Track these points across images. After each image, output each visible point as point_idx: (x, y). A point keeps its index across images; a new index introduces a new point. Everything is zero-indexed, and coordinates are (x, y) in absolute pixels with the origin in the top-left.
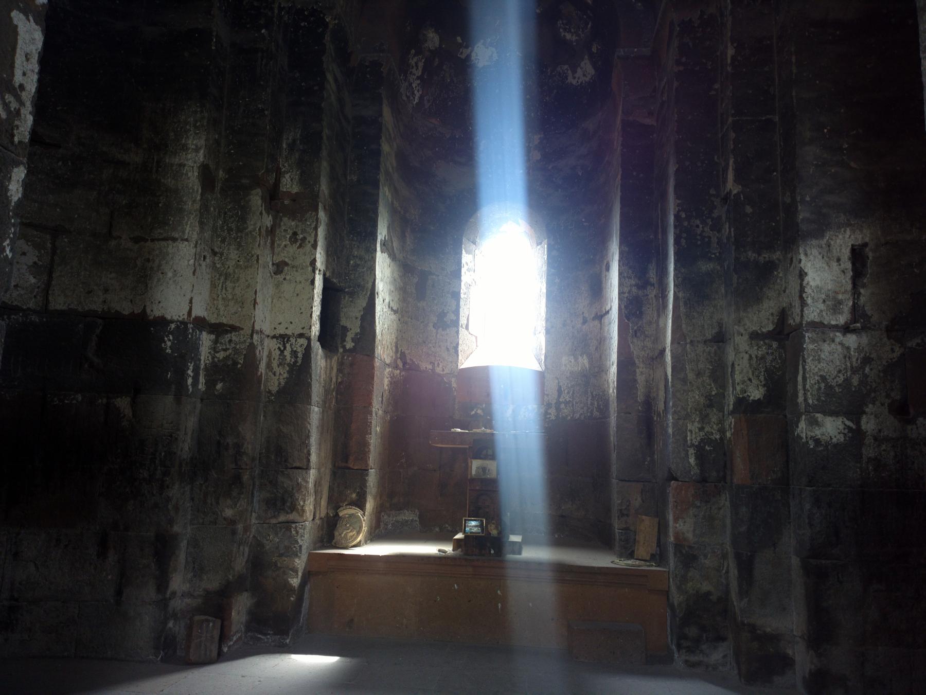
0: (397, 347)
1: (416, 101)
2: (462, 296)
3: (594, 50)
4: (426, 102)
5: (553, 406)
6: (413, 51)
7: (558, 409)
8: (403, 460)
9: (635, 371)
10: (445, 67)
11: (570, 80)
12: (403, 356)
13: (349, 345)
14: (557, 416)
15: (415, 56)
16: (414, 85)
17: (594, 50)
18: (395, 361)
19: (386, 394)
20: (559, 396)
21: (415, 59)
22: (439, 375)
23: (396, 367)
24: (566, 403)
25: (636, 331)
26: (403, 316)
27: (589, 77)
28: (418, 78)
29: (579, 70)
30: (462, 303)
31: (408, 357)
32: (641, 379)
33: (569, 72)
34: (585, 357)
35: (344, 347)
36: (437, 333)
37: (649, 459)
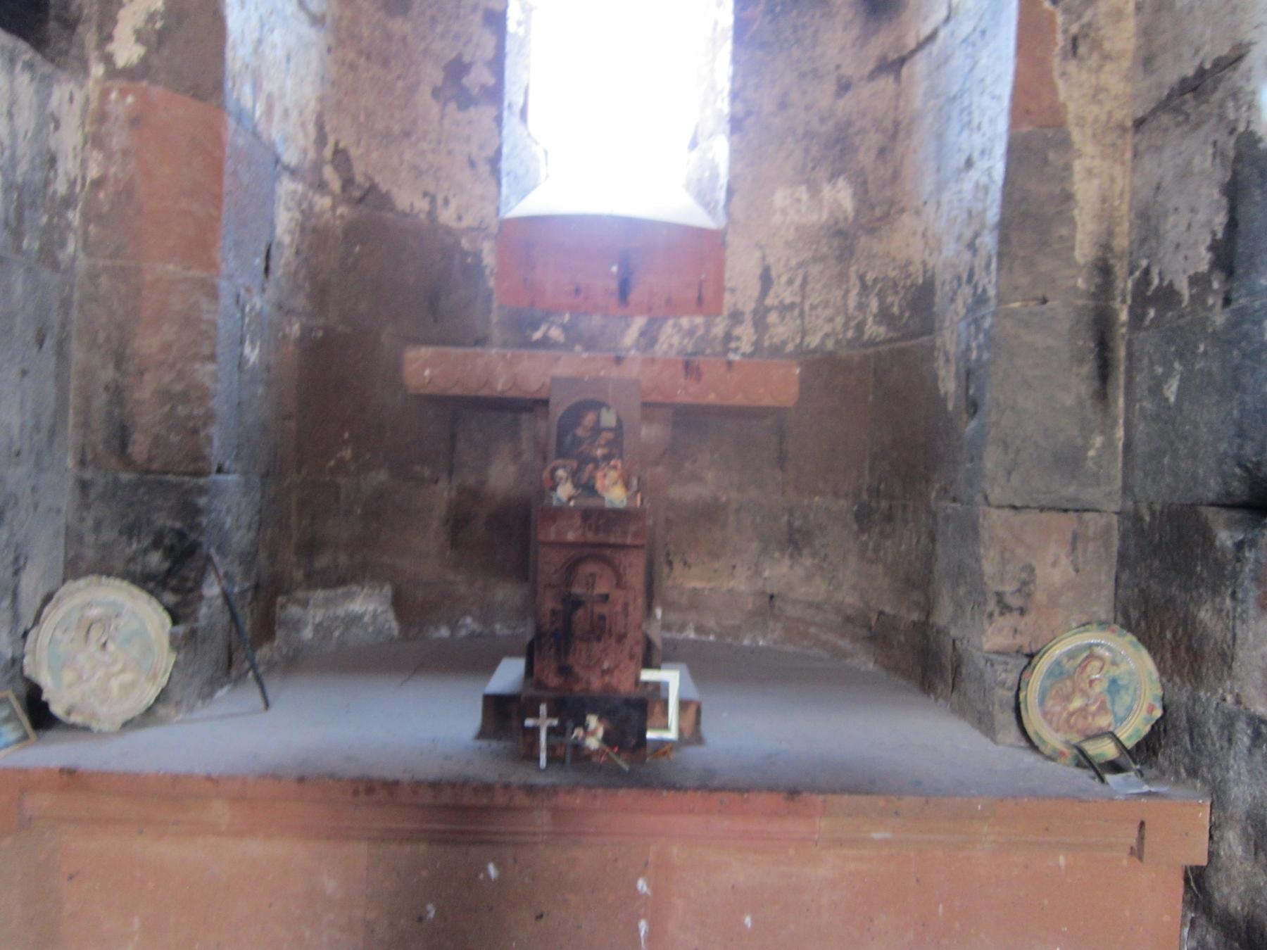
0: (320, 127)
2: (511, 26)
5: (748, 318)
7: (760, 323)
8: (347, 453)
9: (1068, 168)
12: (341, 158)
13: (127, 51)
14: (757, 345)
18: (318, 166)
19: (284, 260)
20: (765, 291)
22: (448, 230)
23: (321, 186)
24: (784, 309)
25: (1075, 42)
26: (340, 43)
30: (510, 45)
31: (359, 170)
32: (1086, 191)
34: (841, 182)
35: (108, 59)
36: (443, 116)
37: (1098, 440)
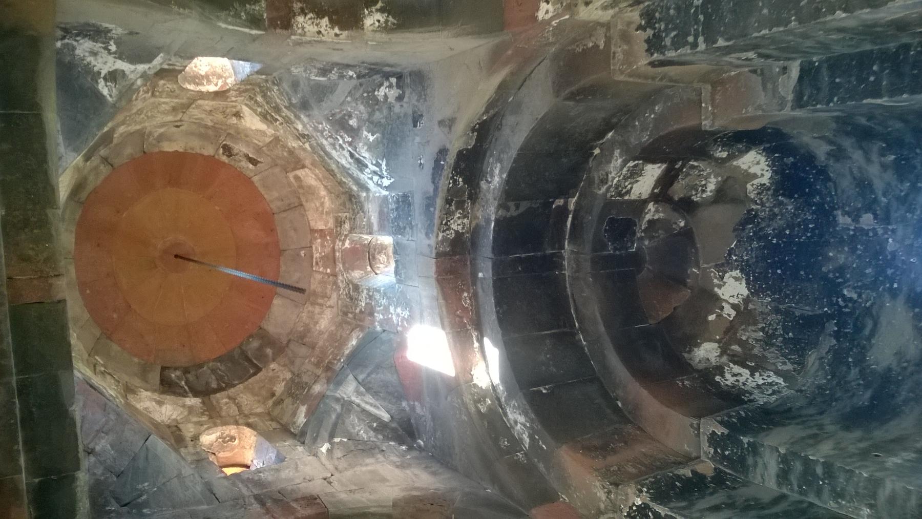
1: (780, 381)
3: (724, 155)
4: (785, 368)
6: (718, 378)
10: (744, 338)
11: (765, 180)
15: (722, 375)
16: (761, 382)
17: (724, 155)
21: (728, 376)
27: (759, 157)
28: (752, 375)
29: (752, 171)
33: (756, 182)
